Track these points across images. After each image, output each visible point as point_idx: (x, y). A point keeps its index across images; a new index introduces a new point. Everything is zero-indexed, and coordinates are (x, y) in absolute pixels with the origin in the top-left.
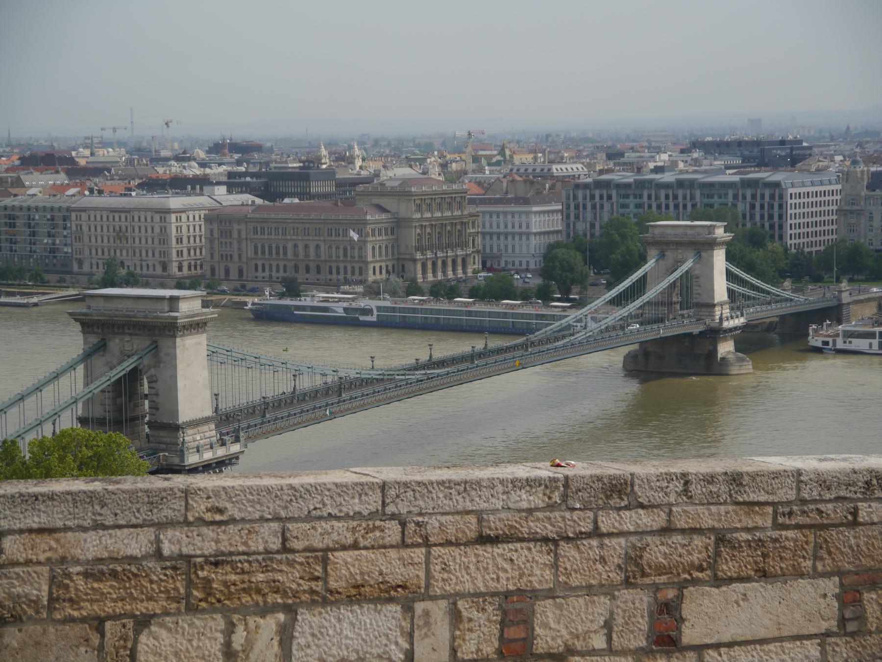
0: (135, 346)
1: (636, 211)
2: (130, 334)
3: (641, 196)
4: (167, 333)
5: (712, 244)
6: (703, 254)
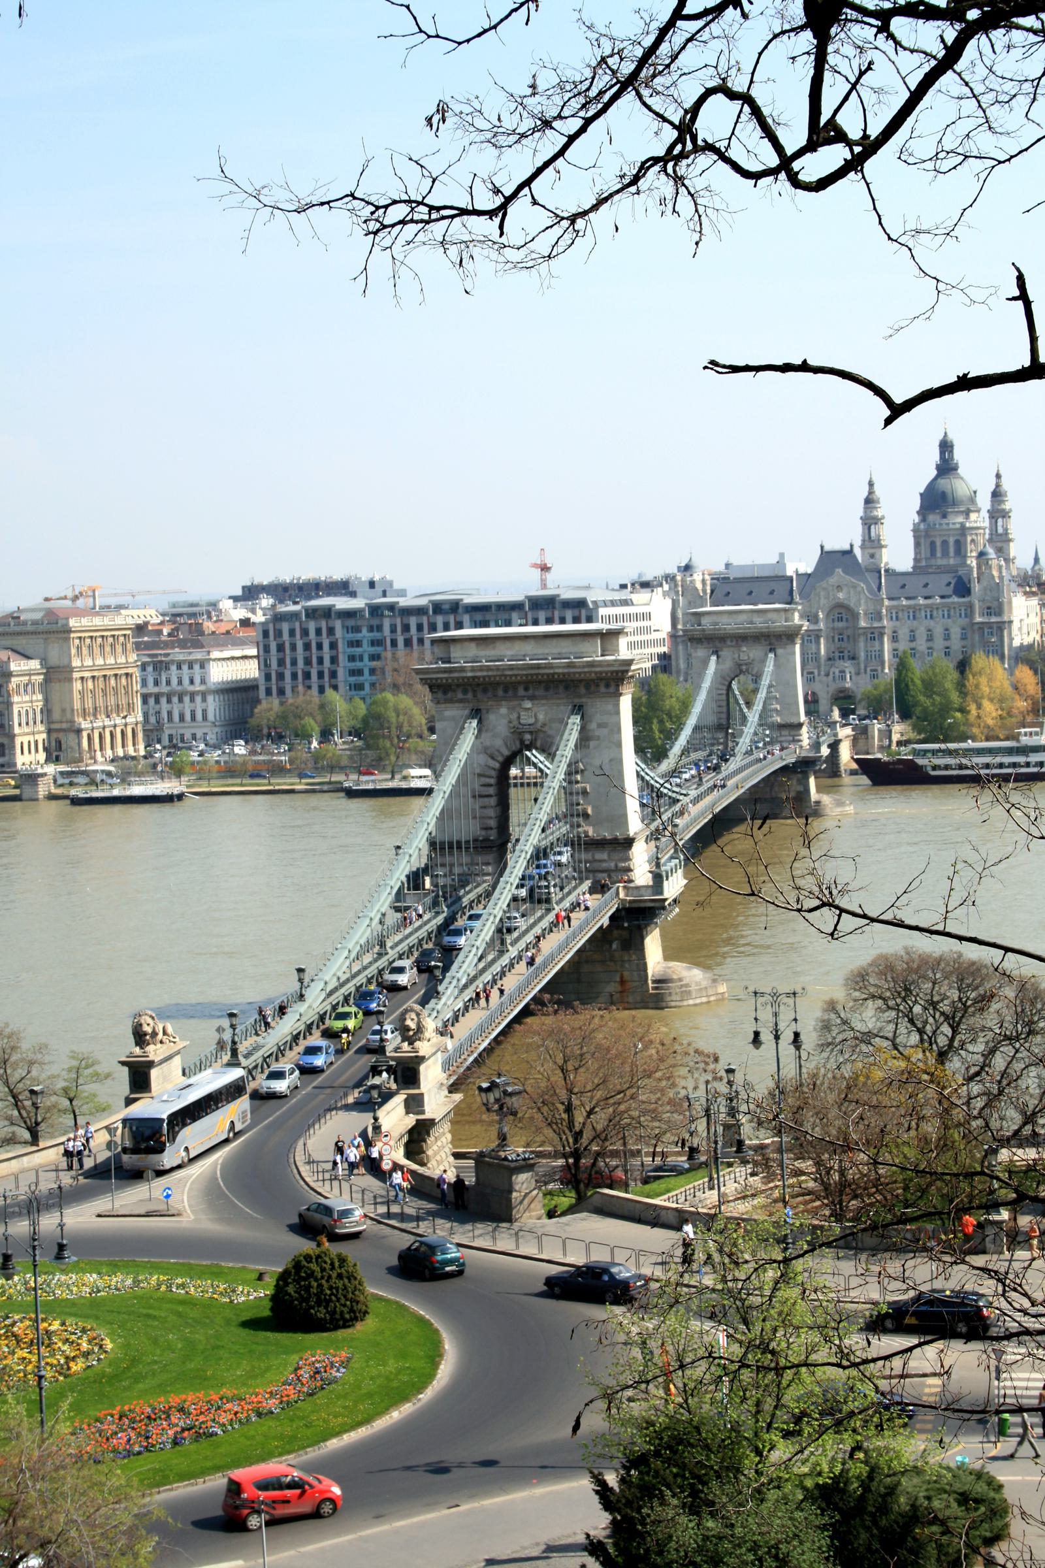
0: (541, 717)
1: (373, 650)
2: (532, 698)
3: (380, 628)
4: (603, 689)
5: (789, 636)
6: (780, 651)
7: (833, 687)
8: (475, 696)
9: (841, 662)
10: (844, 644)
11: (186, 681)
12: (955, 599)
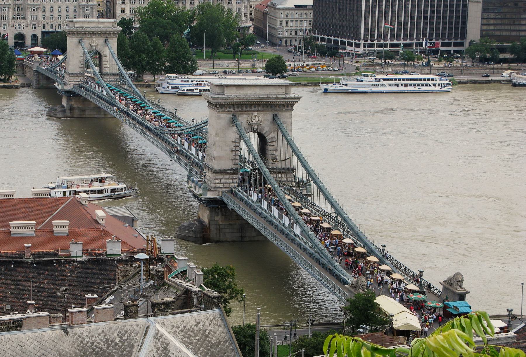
0: (260, 119)
2: (257, 111)
4: (286, 108)
7: (16, 32)
8: (234, 109)
9: (19, 20)
10: (20, 12)
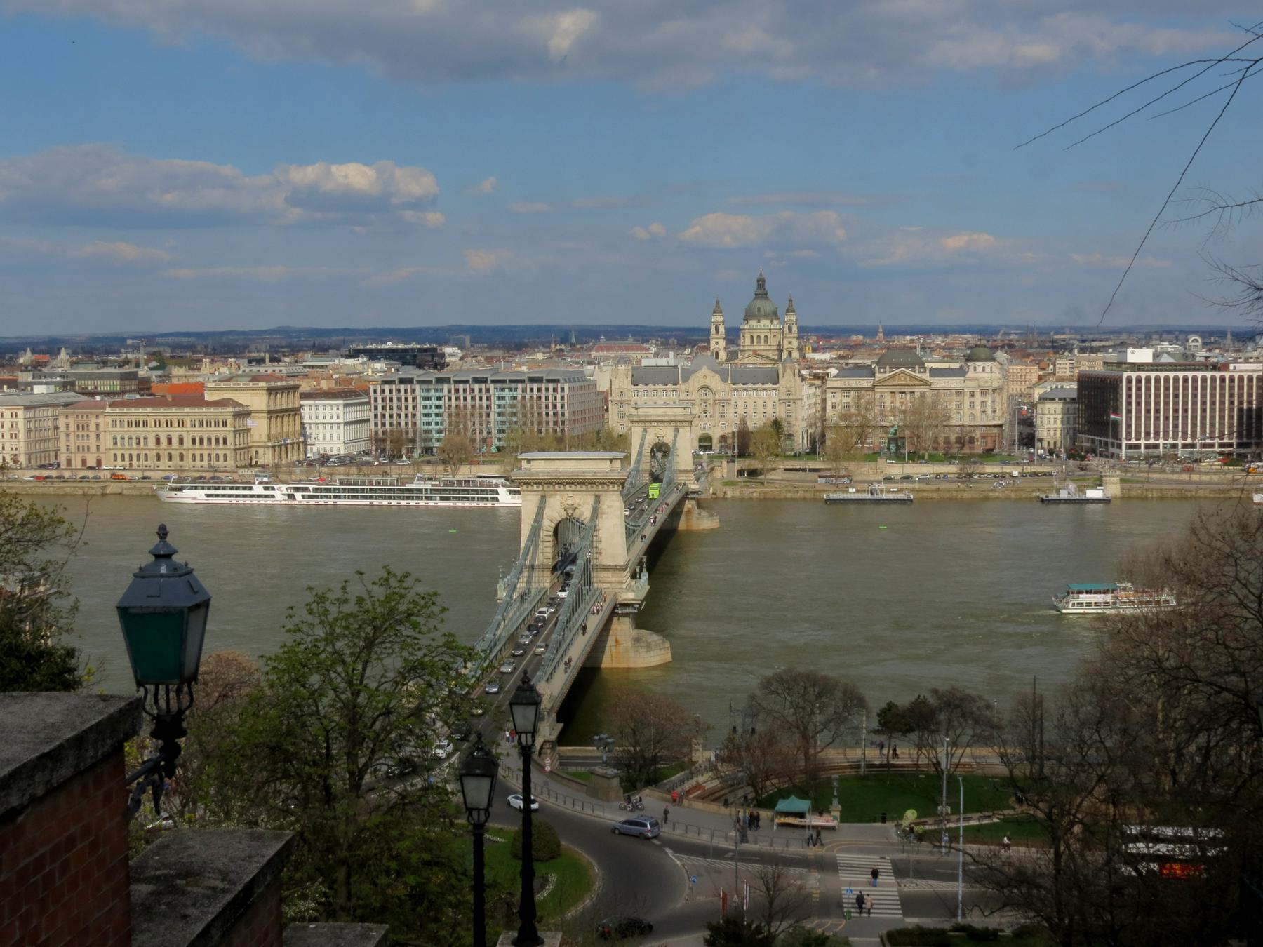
3: (442, 390)
7: (700, 433)
11: (328, 417)
12: (770, 385)
